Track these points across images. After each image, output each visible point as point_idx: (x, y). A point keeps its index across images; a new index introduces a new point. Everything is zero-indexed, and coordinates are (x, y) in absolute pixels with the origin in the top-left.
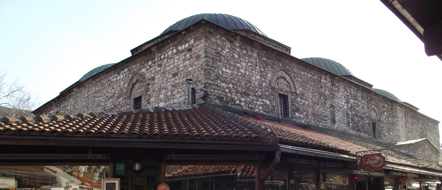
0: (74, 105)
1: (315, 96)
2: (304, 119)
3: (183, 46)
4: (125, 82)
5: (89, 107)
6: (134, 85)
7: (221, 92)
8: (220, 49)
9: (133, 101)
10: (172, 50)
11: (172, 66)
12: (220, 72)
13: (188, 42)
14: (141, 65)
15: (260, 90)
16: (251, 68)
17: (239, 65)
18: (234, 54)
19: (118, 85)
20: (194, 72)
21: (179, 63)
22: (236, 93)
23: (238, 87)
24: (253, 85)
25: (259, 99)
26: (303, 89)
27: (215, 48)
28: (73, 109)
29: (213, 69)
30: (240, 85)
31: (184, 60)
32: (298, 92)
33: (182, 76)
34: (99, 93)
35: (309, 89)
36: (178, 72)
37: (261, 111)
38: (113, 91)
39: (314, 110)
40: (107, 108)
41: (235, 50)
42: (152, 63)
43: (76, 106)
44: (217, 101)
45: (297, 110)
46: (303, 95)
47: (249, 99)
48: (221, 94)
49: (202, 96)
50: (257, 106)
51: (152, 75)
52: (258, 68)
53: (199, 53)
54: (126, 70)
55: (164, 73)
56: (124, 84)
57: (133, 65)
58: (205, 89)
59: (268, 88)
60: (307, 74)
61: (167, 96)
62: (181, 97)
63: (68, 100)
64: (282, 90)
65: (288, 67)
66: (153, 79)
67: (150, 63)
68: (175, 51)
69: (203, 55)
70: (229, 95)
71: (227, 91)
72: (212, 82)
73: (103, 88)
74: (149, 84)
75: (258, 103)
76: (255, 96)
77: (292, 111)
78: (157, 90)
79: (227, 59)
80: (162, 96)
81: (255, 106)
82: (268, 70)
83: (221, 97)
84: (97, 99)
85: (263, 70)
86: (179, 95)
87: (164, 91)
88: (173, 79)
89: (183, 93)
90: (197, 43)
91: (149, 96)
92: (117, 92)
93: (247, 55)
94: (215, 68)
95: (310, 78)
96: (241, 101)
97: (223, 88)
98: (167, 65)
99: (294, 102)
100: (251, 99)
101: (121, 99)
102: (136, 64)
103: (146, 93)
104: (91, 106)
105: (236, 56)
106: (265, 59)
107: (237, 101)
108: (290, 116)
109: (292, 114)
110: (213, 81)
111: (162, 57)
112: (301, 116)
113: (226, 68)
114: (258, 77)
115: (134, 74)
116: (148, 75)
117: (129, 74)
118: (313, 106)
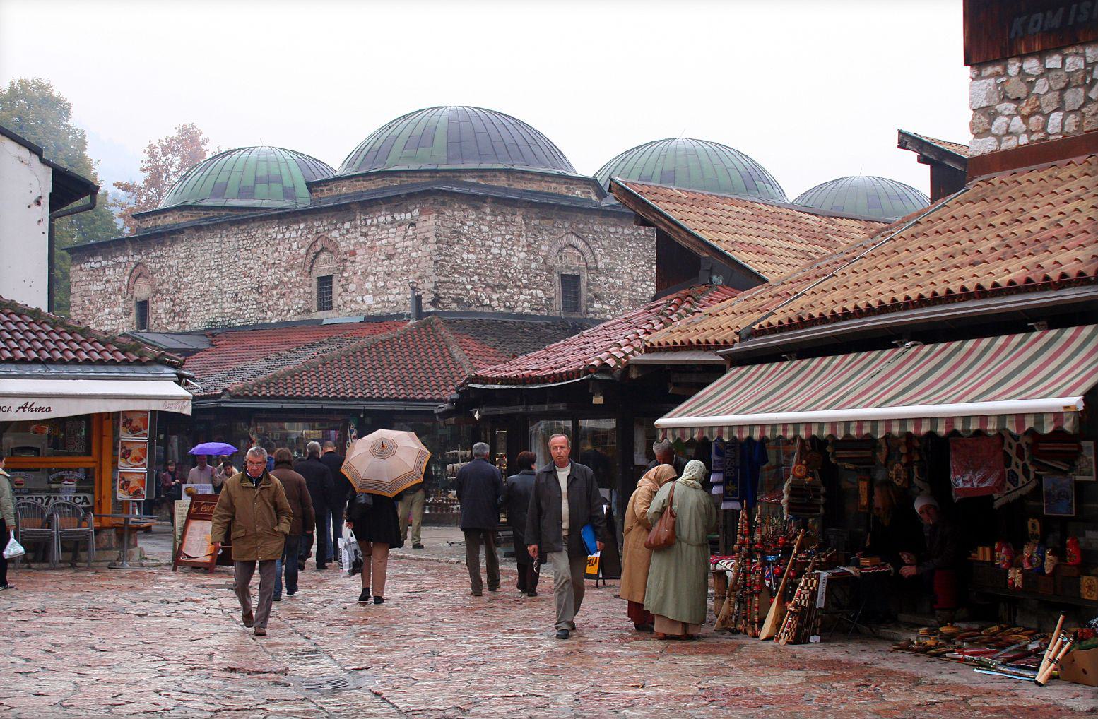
0: (185, 260)
1: (638, 267)
2: (613, 313)
3: (403, 215)
4: (300, 246)
5: (225, 274)
6: (317, 254)
7: (459, 292)
8: (459, 225)
9: (315, 282)
10: (386, 215)
11: (385, 241)
12: (459, 261)
13: (411, 211)
14: (331, 224)
15: (525, 275)
16: (510, 243)
17: (491, 243)
18: (482, 227)
19: (287, 246)
20: (420, 262)
21: (396, 240)
22: (484, 289)
23: (488, 278)
24: (513, 271)
25: (523, 292)
26: (611, 259)
27: (451, 225)
28: (183, 267)
29: (447, 258)
30: (491, 274)
31: (404, 239)
32: (601, 265)
33: (402, 263)
34: (246, 252)
35: (625, 256)
36: (395, 254)
37: (526, 311)
38: (276, 254)
39: (634, 293)
40: (264, 283)
41: (483, 220)
42: (351, 227)
43: (192, 264)
44: (454, 305)
45: (599, 298)
46: (612, 270)
47: (506, 294)
48: (460, 294)
49: (430, 300)
50: (520, 303)
51: (352, 247)
52: (523, 239)
53: (428, 235)
54: (302, 226)
55: (369, 248)
56: (298, 248)
57: (317, 220)
58: (436, 292)
59: (541, 270)
60: (623, 228)
61: (376, 286)
62: (399, 294)
63: (170, 246)
64: (569, 268)
65: (581, 226)
66: (353, 253)
67: (347, 225)
68: (389, 219)
69: (433, 239)
70: (473, 293)
71: (469, 287)
72: (446, 279)
73: (255, 245)
74: (344, 260)
75: (522, 297)
76: (517, 286)
77: (588, 301)
78: (360, 273)
79: (470, 238)
80: (368, 285)
81: (516, 303)
82: (543, 240)
83: (459, 299)
84: (241, 262)
85: (532, 241)
86: (397, 291)
87: (371, 278)
88: (386, 263)
89: (402, 289)
90: (424, 217)
91: (346, 279)
92: (284, 259)
93: (504, 223)
94: (451, 256)
95: (628, 235)
96: (491, 300)
97: (464, 284)
98: (377, 237)
99: (592, 285)
100: (509, 293)
101: (294, 273)
102: (321, 219)
103: (341, 274)
104: (229, 272)
105: (485, 229)
106: (537, 222)
107: (485, 301)
108: (583, 310)
109: (587, 306)
110: (447, 276)
111: (369, 222)
112: (606, 307)
113: (469, 252)
114: (523, 255)
115: (317, 236)
116: (344, 246)
117: (309, 233)
118: (632, 286)
